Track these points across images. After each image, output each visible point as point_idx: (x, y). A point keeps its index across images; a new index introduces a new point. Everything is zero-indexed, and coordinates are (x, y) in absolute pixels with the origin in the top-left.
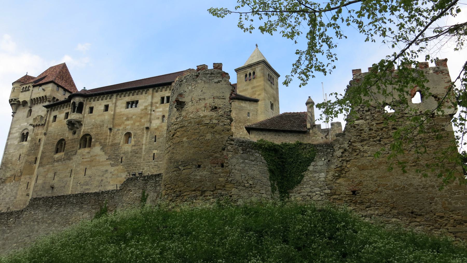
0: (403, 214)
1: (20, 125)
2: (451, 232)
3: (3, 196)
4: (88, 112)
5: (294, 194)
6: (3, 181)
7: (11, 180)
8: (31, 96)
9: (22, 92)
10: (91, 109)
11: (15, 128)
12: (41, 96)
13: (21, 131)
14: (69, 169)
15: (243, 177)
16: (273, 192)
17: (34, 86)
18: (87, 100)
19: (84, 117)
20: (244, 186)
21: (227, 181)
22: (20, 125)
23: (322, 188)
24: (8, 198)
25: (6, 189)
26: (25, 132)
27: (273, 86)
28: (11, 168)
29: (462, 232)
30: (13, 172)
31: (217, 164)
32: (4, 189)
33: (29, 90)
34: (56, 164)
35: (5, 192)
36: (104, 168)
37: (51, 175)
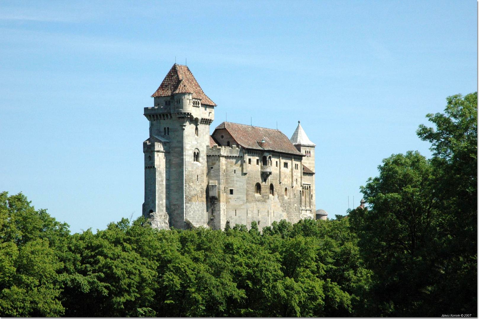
3: (193, 214)
28: (193, 187)
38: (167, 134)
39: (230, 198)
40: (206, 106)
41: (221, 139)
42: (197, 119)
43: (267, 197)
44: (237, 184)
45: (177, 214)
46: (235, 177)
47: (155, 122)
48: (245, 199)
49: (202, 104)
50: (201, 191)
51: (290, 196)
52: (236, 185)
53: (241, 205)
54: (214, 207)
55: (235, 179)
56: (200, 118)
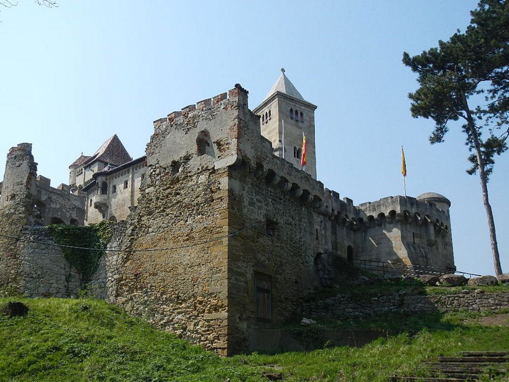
0: (171, 301)
2: (205, 320)
4: (111, 192)
5: (94, 281)
8: (84, 179)
9: (77, 176)
10: (115, 187)
15: (32, 267)
16: (68, 281)
17: (85, 168)
18: (110, 179)
19: (109, 197)
20: (32, 277)
21: (18, 274)
23: (114, 273)
27: (300, 124)
29: (215, 320)
31: (11, 256)
33: (82, 173)
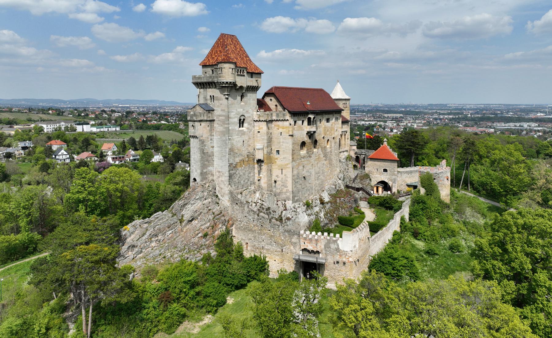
1: (236, 110)
3: (238, 179)
6: (234, 166)
7: (241, 164)
11: (232, 112)
12: (254, 85)
13: (239, 116)
14: (311, 164)
22: (236, 110)
24: (242, 181)
25: (239, 173)
26: (242, 118)
30: (241, 158)
32: (237, 173)
34: (303, 160)
35: (239, 176)
36: (323, 163)
37: (301, 168)
38: (212, 102)
39: (277, 159)
40: (252, 74)
41: (270, 101)
42: (241, 87)
43: (311, 153)
44: (282, 145)
45: (222, 181)
46: (281, 139)
47: (202, 90)
48: (291, 158)
49: (248, 73)
50: (248, 155)
51: (331, 145)
52: (282, 147)
53: (287, 164)
54: (261, 169)
55: (281, 140)
56: (245, 86)
